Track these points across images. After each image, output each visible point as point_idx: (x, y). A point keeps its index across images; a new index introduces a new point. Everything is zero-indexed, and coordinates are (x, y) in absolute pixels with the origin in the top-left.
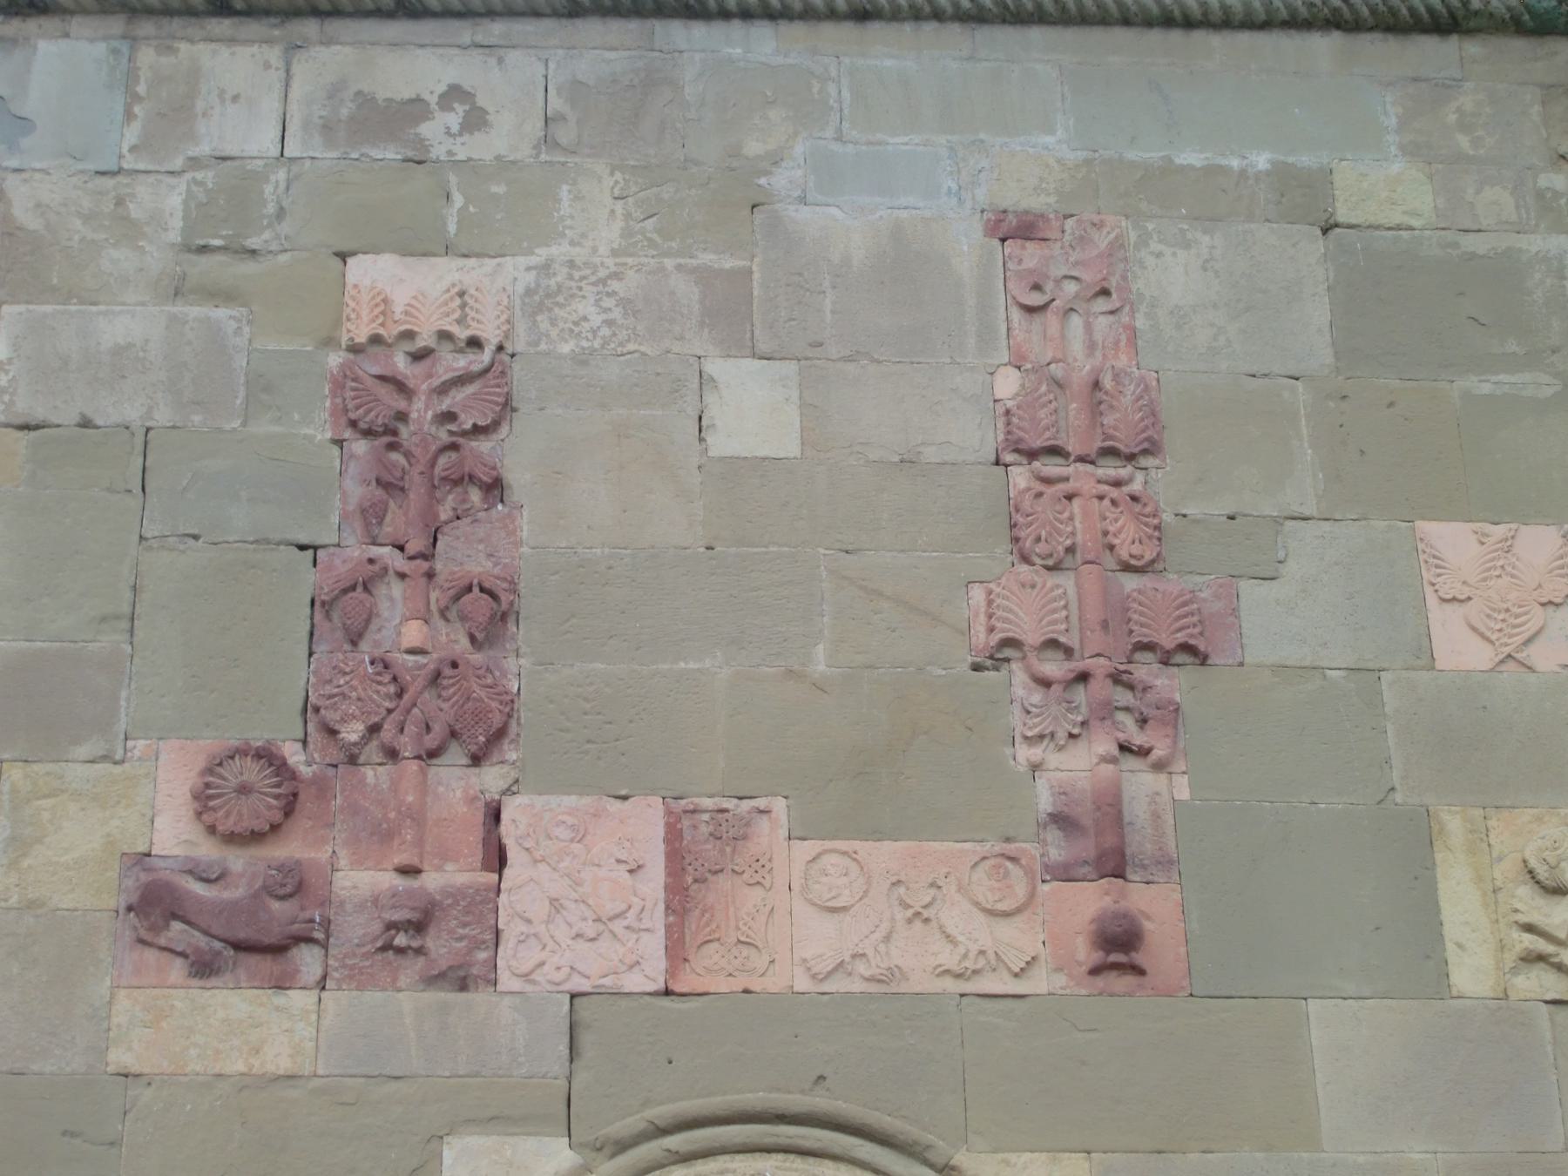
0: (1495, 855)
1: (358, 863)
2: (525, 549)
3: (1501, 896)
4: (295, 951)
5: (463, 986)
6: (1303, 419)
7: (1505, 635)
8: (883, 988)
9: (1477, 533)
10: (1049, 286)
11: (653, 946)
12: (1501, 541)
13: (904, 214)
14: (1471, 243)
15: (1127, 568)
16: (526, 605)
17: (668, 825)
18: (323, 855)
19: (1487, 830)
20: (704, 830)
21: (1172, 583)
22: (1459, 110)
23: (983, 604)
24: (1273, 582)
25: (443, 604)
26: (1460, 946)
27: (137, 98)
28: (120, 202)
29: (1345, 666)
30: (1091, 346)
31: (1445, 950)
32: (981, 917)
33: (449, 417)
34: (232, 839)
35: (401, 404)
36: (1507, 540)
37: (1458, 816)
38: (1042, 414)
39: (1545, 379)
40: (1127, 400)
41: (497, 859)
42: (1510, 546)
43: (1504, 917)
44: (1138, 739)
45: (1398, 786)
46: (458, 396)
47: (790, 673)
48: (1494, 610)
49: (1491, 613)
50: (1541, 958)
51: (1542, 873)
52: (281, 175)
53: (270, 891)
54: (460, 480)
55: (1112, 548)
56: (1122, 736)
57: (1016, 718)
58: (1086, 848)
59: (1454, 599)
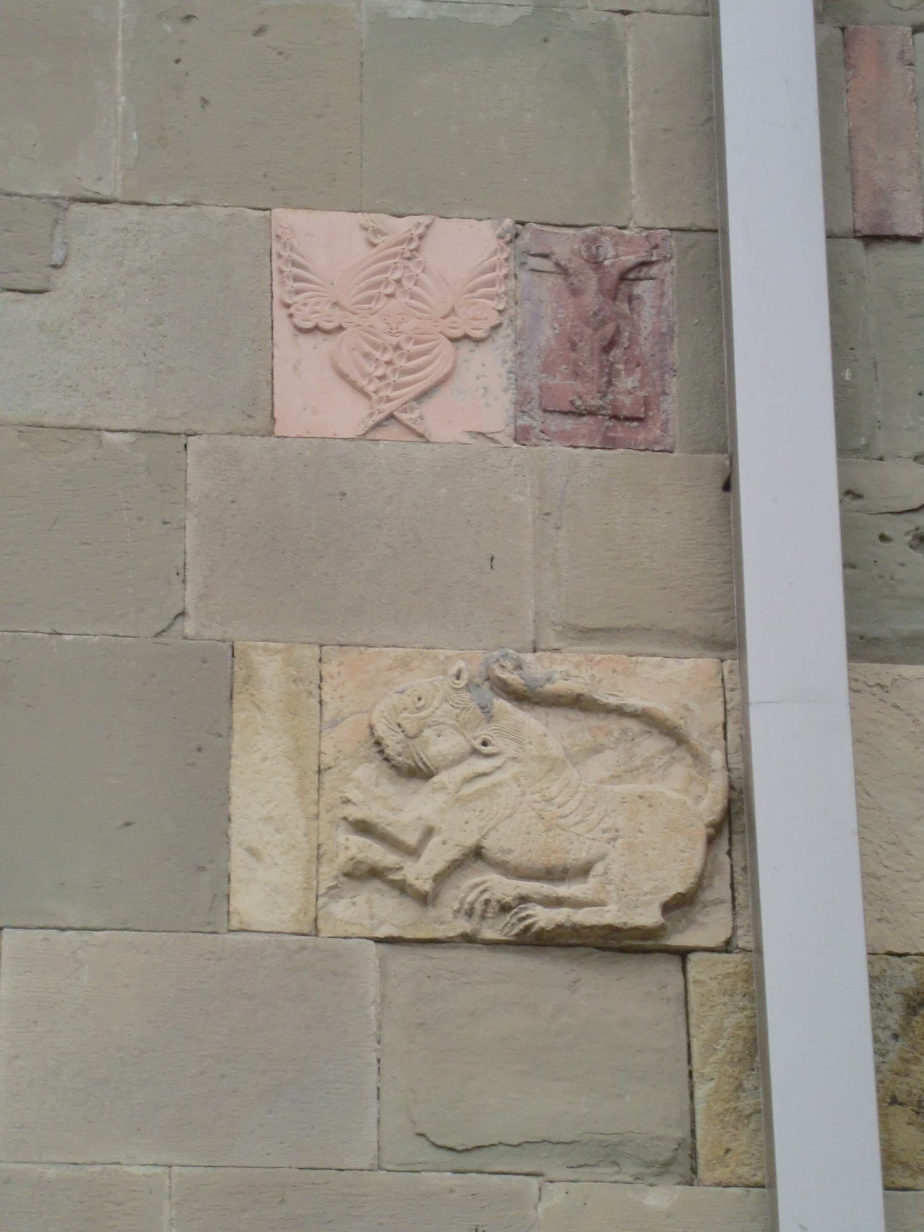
0: (327, 716)
3: (327, 778)
6: (120, 50)
7: (389, 384)
9: (366, 229)
12: (400, 243)
19: (321, 679)
24: (40, 296)
26: (253, 852)
29: (134, 426)
31: (228, 859)
36: (411, 240)
37: (279, 658)
42: (417, 249)
43: (328, 811)
45: (190, 610)
48: (376, 346)
49: (374, 352)
50: (375, 873)
51: (393, 746)
59: (316, 329)
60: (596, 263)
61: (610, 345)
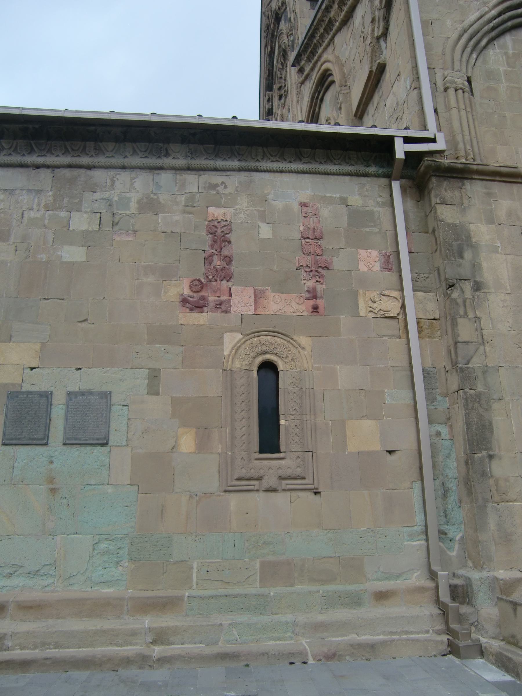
1: (212, 296)
2: (234, 251)
4: (204, 308)
5: (226, 313)
8: (283, 314)
10: (308, 214)
11: (252, 308)
13: (287, 202)
14: (368, 209)
15: (318, 255)
16: (234, 259)
17: (254, 291)
18: (207, 294)
20: (259, 292)
21: (324, 258)
22: (366, 189)
23: (298, 260)
25: (223, 259)
27: (177, 183)
28: (175, 199)
30: (313, 223)
32: (297, 304)
33: (223, 231)
34: (195, 292)
35: (216, 230)
38: (306, 233)
39: (376, 229)
40: (318, 231)
41: (231, 295)
44: (319, 280)
46: (224, 228)
47: (271, 270)
50: (372, 311)
52: (198, 195)
53: (200, 299)
54: (225, 241)
55: (316, 252)
56: (317, 279)
57: (302, 276)
58: (311, 295)
60: (386, 255)
61: (388, 262)
